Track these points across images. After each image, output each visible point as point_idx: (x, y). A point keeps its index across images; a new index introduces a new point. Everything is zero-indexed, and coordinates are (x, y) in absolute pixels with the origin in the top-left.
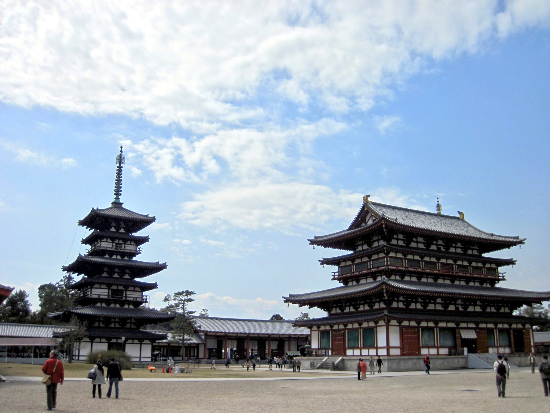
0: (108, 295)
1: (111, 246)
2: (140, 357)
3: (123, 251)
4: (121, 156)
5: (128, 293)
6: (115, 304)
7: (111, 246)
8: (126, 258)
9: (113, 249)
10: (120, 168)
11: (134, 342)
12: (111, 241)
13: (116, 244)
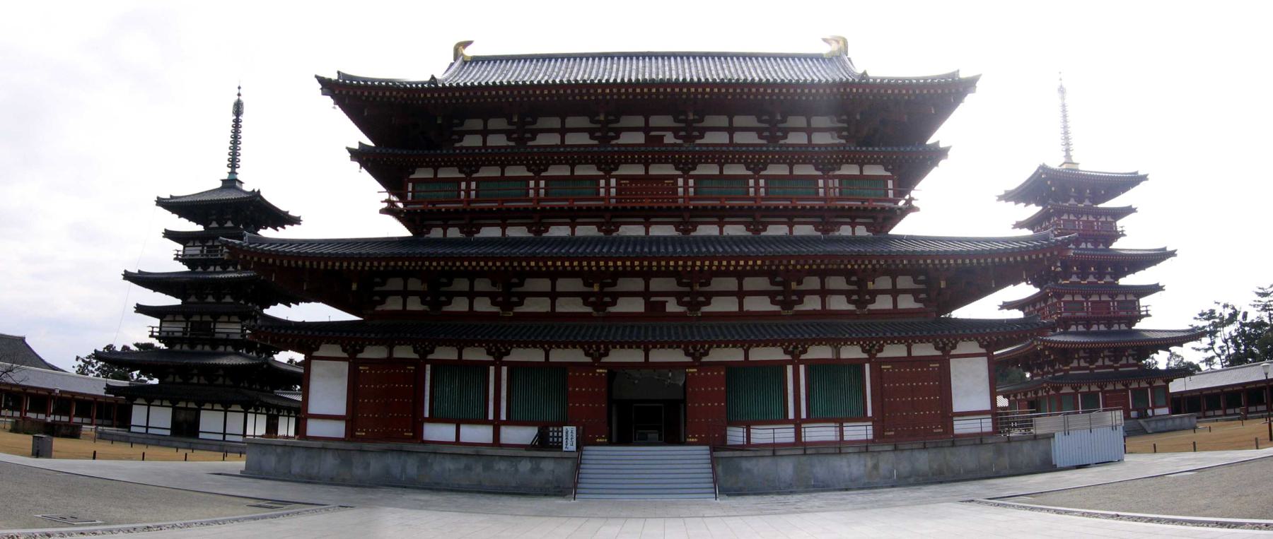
0: (184, 333)
1: (198, 252)
2: (224, 434)
3: (219, 256)
4: (239, 99)
5: (218, 326)
6: (204, 345)
7: (198, 252)
8: (200, 269)
9: (205, 257)
10: (237, 124)
11: (215, 408)
12: (200, 244)
13: (208, 247)
